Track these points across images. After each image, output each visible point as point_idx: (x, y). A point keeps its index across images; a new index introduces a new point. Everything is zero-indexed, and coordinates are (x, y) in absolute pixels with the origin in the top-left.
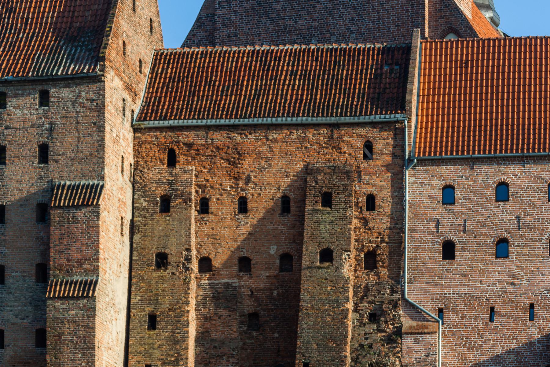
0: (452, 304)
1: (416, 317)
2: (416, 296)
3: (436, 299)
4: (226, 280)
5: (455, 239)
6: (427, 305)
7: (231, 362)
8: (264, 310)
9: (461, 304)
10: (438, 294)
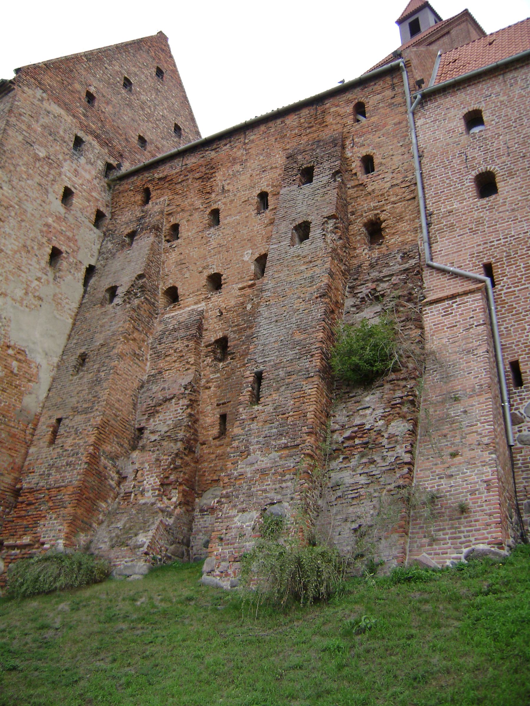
0: (505, 253)
1: (449, 286)
2: (446, 257)
3: (477, 253)
4: (192, 307)
5: (491, 168)
6: (465, 265)
7: (181, 404)
8: (234, 332)
9: (520, 249)
10: (480, 245)
